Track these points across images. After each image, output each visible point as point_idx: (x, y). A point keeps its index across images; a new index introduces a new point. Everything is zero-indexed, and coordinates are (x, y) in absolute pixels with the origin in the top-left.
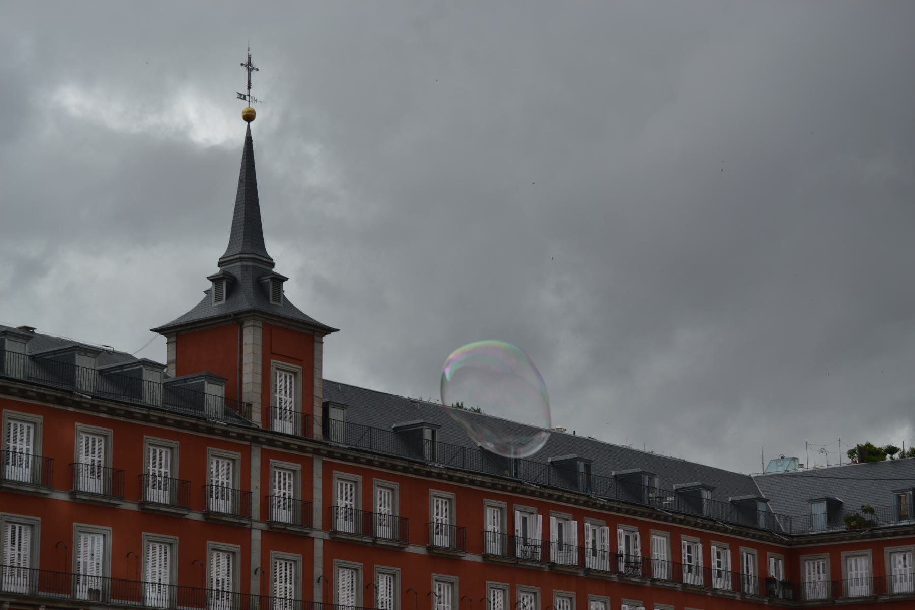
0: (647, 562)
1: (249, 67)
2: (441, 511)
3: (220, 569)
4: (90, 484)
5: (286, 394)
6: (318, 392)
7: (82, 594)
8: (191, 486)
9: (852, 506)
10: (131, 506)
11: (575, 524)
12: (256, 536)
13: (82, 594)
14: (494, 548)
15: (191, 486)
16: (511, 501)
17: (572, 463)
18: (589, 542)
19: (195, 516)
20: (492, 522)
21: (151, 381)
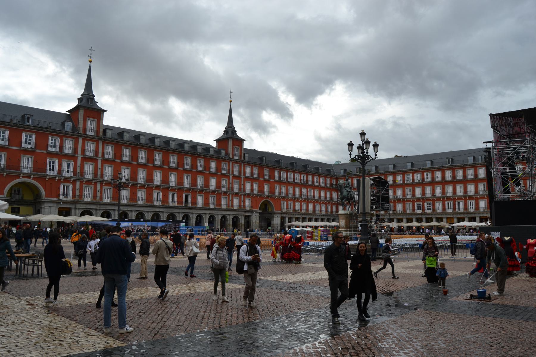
0: (307, 181)
1: (231, 92)
2: (266, 172)
3: (224, 183)
4: (200, 168)
5: (237, 152)
6: (243, 151)
7: (199, 187)
8: (219, 169)
9: (348, 171)
10: (208, 172)
11: (293, 174)
12: (231, 177)
13: (199, 187)
14: (277, 178)
15: (219, 169)
16: (280, 170)
17: (293, 163)
18: (296, 177)
19: (219, 174)
20: (276, 174)
21: (211, 149)
